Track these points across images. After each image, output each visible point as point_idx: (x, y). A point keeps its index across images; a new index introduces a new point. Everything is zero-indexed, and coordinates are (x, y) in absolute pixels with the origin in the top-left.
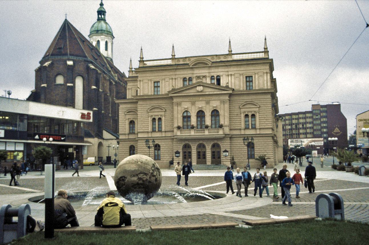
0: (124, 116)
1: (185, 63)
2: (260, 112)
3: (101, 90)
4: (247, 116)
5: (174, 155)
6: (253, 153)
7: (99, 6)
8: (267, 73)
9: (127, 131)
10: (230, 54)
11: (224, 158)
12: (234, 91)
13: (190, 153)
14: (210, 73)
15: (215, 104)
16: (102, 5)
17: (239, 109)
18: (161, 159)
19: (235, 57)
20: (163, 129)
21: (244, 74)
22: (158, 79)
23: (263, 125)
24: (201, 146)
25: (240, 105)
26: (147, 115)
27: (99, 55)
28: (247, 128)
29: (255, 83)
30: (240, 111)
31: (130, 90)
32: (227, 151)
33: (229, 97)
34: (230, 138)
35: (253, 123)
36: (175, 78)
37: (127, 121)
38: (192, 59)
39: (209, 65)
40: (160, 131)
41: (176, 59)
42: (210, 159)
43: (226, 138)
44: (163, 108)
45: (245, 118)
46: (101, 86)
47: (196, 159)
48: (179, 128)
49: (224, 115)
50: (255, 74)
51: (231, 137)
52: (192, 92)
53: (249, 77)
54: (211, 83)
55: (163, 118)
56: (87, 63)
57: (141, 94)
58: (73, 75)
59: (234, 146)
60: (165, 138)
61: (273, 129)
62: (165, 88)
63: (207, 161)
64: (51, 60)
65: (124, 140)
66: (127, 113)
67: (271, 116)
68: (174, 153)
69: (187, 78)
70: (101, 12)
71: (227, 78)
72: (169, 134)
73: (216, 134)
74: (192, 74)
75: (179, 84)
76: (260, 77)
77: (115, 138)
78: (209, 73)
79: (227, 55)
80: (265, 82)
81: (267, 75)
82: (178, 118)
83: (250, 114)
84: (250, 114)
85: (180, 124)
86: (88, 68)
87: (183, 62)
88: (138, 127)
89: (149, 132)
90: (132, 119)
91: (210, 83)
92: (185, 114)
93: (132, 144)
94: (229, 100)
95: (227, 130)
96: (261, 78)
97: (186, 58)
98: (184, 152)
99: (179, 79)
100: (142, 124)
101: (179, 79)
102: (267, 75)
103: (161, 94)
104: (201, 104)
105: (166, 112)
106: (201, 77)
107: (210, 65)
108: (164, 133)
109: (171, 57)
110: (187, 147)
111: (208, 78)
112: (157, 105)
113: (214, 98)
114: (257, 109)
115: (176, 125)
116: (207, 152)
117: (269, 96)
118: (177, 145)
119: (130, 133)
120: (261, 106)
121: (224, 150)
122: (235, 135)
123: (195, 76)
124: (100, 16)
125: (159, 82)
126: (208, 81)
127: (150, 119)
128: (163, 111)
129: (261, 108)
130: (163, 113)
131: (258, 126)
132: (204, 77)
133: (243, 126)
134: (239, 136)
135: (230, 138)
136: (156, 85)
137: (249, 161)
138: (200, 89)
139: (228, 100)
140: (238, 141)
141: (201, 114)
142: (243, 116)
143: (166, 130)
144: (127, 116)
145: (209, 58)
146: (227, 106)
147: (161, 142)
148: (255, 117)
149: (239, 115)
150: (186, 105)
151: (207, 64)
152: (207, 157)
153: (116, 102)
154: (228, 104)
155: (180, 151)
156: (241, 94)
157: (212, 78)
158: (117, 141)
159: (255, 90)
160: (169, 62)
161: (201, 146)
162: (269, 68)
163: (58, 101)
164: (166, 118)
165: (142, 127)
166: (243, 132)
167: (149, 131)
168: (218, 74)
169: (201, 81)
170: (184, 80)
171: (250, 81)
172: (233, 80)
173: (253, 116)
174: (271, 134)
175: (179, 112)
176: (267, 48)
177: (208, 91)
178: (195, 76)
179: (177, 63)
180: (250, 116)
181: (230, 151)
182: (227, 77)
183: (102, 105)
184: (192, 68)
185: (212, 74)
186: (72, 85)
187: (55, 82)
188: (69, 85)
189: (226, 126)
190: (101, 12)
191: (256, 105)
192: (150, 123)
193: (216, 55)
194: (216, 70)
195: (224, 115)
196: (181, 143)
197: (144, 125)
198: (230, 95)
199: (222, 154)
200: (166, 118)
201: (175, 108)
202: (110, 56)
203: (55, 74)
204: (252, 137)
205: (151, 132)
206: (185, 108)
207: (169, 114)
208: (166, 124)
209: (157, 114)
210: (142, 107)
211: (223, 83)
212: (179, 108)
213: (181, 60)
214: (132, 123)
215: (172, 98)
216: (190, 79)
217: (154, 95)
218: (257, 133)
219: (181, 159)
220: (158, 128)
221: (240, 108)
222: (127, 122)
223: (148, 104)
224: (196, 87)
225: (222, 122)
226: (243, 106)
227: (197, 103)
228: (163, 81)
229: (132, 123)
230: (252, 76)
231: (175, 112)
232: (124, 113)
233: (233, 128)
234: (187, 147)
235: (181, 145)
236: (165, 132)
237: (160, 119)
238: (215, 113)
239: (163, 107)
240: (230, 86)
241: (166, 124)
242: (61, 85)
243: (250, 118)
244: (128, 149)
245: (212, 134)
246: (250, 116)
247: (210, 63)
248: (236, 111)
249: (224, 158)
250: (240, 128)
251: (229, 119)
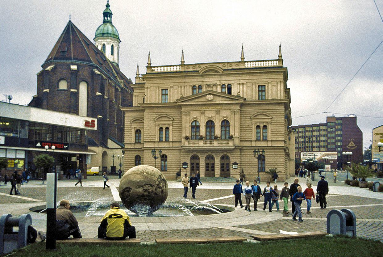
0: (130, 125)
1: (195, 70)
2: (272, 124)
3: (106, 97)
4: (258, 127)
5: (182, 166)
6: (263, 166)
7: (106, 8)
8: (281, 82)
9: (133, 140)
10: (243, 61)
11: (233, 171)
12: (245, 101)
13: (198, 164)
14: (221, 81)
15: (225, 114)
16: (108, 6)
17: (250, 120)
18: (168, 171)
19: (248, 65)
20: (171, 139)
21: (256, 83)
22: (166, 87)
23: (275, 137)
24: (210, 158)
25: (251, 115)
26: (155, 124)
27: (105, 60)
28: (258, 140)
29: (268, 92)
30: (251, 122)
31: (137, 98)
32: (237, 164)
33: (240, 107)
34: (241, 149)
35: (265, 134)
36: (184, 86)
37: (133, 130)
38: (202, 66)
39: (220, 72)
40: (167, 141)
41: (185, 65)
42: (219, 171)
43: (236, 150)
44: (171, 117)
45: (256, 129)
46: (106, 92)
47: (204, 171)
48: (187, 138)
49: (235, 126)
50: (268, 83)
51: (241, 149)
52: (201, 101)
53: (262, 86)
54: (222, 92)
55: (171, 128)
56: (91, 67)
57: (149, 102)
58: (76, 80)
59: (244, 158)
60: (173, 149)
61: (285, 142)
62: (173, 96)
63: (216, 173)
64: (53, 64)
65: (130, 150)
66: (133, 121)
67: (283, 128)
68: (182, 164)
69: (197, 86)
70: (107, 14)
71: (239, 87)
72: (177, 145)
73: (226, 145)
74: (202, 82)
75: (188, 92)
76: (273, 86)
77: (121, 147)
78: (219, 81)
79: (239, 62)
80: (279, 92)
81: (281, 85)
82: (186, 128)
83: (262, 125)
84: (262, 125)
85: (189, 134)
86: (93, 73)
87: (193, 68)
88: (145, 137)
89: (156, 142)
90: (138, 128)
91: (220, 91)
92: (194, 124)
93: (138, 154)
94: (240, 110)
95: (237, 142)
96: (274, 88)
97: (196, 64)
98: (192, 164)
99: (188, 87)
100: (148, 133)
101: (188, 87)
102: (281, 85)
103: (169, 102)
104: (210, 114)
105: (173, 122)
106: (212, 85)
107: (221, 73)
108: (171, 144)
109: (180, 63)
110: (195, 158)
111: (218, 87)
112: (164, 113)
114: (270, 120)
115: (184, 135)
116: (216, 164)
117: (282, 107)
118: (185, 156)
119: (135, 143)
120: (273, 117)
121: (233, 162)
122: (245, 147)
123: (205, 84)
124: (106, 18)
125: (167, 89)
126: (219, 89)
127: (157, 128)
128: (170, 120)
129: (273, 119)
131: (269, 138)
132: (215, 85)
133: (254, 138)
134: (250, 148)
135: (241, 149)
136: (164, 93)
137: (259, 175)
138: (210, 98)
139: (239, 110)
140: (249, 154)
141: (210, 124)
142: (254, 127)
143: (173, 140)
144: (133, 124)
145: (220, 65)
146: (238, 116)
147: (168, 152)
148: (267, 129)
149: (251, 126)
150: (195, 114)
151: (218, 72)
152: (216, 169)
153: (121, 110)
154: (239, 114)
155: (187, 162)
156: (253, 104)
157: (223, 86)
158: (122, 151)
159: (268, 100)
160: (178, 69)
161: (210, 158)
162: (283, 77)
163: (61, 107)
164: (174, 128)
165: (148, 136)
166: (253, 144)
167: (156, 141)
169: (211, 89)
170: (194, 87)
171: (262, 91)
172: (245, 89)
173: (265, 127)
174: (283, 146)
175: (188, 121)
176: (281, 56)
177: (219, 100)
179: (187, 70)
180: (262, 127)
181: (240, 163)
182: (239, 85)
183: (106, 112)
184: (202, 76)
185: (223, 83)
186: (76, 90)
187: (58, 88)
188: (72, 90)
189: (236, 137)
190: (107, 14)
191: (268, 116)
192: (157, 132)
193: (228, 63)
194: (227, 78)
195: (235, 126)
196: (189, 155)
197: (150, 134)
198: (242, 105)
199: (231, 167)
200: (174, 128)
201: (184, 117)
202: (116, 61)
203: (58, 79)
204: (263, 149)
205: (158, 142)
206: (194, 118)
207: (177, 123)
208: (174, 134)
209: (164, 123)
210: (149, 116)
211: (234, 92)
212: (188, 118)
213: (191, 67)
214: (138, 132)
215: (180, 106)
216: (200, 87)
217: (162, 103)
218: (269, 145)
219: (189, 171)
220: (166, 137)
221: (252, 119)
222: (133, 131)
223: (155, 113)
224: (206, 95)
225: (232, 133)
226: (254, 117)
227: (206, 112)
228: (172, 89)
229: (138, 132)
230: (265, 86)
231: (183, 122)
232: (130, 122)
233: (244, 140)
234: (195, 158)
235: (189, 156)
236: (173, 142)
237: (167, 129)
238: (225, 124)
239: (171, 116)
240: (241, 96)
241: (174, 134)
242: (64, 90)
243: (262, 130)
244: (134, 159)
245: (222, 145)
246: (262, 127)
247: (221, 71)
248: (248, 122)
249: (233, 171)
250: (251, 139)
251: (239, 130)
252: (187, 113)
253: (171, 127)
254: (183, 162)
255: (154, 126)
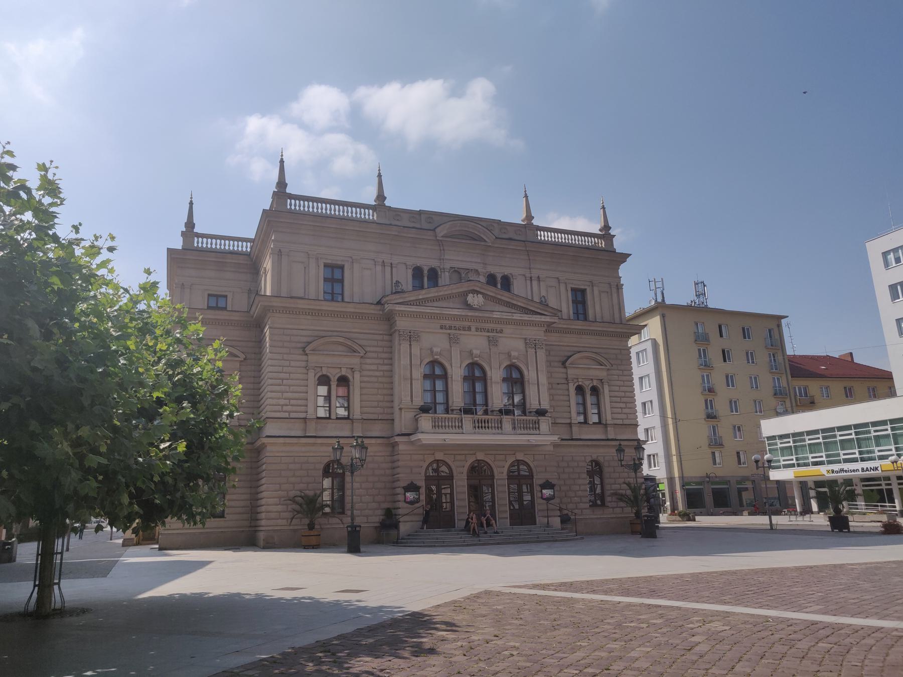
5: (401, 497)
55: (356, 380)
71: (529, 287)
82: (411, 379)
100: (282, 392)
113: (508, 329)
130: (355, 361)
138: (476, 303)
141: (476, 375)
155: (419, 484)
165: (282, 402)
168: (507, 271)
170: (418, 272)
178: (447, 266)
182: (528, 282)
197: (290, 395)
200: (366, 379)
207: (374, 367)
216: (434, 275)
231: (402, 361)
252: (412, 337)
253: (357, 376)
254: (405, 485)
255: (305, 371)
